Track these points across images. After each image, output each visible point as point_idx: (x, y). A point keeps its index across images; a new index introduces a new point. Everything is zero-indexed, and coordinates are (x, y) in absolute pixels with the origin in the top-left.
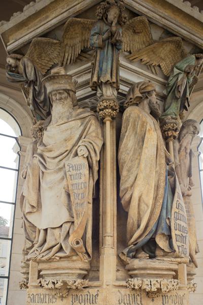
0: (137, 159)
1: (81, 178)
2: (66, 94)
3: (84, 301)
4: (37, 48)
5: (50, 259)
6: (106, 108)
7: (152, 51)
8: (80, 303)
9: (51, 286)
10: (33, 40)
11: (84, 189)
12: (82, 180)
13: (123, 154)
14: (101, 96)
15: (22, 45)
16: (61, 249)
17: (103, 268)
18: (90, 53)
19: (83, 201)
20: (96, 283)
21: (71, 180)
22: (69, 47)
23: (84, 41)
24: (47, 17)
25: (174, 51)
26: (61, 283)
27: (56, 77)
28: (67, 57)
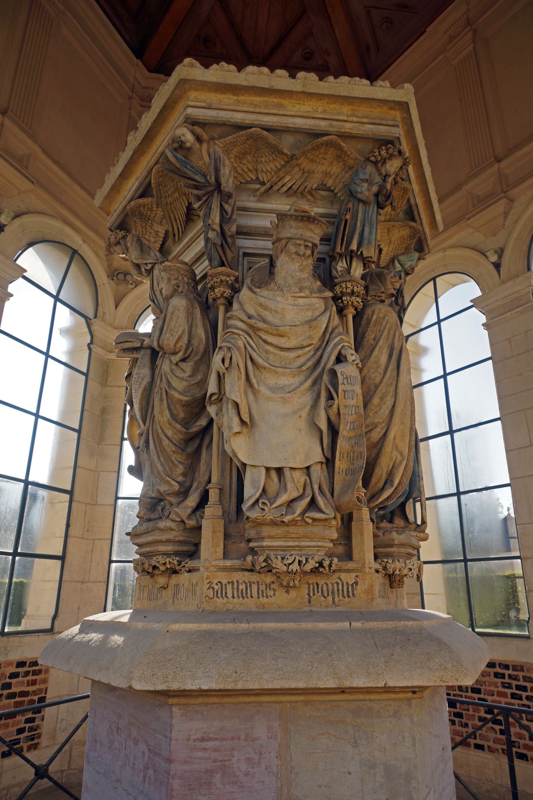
0: (392, 384)
1: (353, 399)
2: (309, 252)
4: (249, 142)
5: (292, 521)
6: (353, 293)
7: (388, 229)
8: (324, 597)
9: (295, 567)
11: (354, 416)
12: (353, 402)
13: (372, 371)
14: (341, 271)
16: (313, 504)
17: (363, 541)
20: (350, 565)
21: (345, 398)
22: (300, 169)
25: (404, 239)
26: (316, 562)
27: (316, 222)
28: (286, 180)
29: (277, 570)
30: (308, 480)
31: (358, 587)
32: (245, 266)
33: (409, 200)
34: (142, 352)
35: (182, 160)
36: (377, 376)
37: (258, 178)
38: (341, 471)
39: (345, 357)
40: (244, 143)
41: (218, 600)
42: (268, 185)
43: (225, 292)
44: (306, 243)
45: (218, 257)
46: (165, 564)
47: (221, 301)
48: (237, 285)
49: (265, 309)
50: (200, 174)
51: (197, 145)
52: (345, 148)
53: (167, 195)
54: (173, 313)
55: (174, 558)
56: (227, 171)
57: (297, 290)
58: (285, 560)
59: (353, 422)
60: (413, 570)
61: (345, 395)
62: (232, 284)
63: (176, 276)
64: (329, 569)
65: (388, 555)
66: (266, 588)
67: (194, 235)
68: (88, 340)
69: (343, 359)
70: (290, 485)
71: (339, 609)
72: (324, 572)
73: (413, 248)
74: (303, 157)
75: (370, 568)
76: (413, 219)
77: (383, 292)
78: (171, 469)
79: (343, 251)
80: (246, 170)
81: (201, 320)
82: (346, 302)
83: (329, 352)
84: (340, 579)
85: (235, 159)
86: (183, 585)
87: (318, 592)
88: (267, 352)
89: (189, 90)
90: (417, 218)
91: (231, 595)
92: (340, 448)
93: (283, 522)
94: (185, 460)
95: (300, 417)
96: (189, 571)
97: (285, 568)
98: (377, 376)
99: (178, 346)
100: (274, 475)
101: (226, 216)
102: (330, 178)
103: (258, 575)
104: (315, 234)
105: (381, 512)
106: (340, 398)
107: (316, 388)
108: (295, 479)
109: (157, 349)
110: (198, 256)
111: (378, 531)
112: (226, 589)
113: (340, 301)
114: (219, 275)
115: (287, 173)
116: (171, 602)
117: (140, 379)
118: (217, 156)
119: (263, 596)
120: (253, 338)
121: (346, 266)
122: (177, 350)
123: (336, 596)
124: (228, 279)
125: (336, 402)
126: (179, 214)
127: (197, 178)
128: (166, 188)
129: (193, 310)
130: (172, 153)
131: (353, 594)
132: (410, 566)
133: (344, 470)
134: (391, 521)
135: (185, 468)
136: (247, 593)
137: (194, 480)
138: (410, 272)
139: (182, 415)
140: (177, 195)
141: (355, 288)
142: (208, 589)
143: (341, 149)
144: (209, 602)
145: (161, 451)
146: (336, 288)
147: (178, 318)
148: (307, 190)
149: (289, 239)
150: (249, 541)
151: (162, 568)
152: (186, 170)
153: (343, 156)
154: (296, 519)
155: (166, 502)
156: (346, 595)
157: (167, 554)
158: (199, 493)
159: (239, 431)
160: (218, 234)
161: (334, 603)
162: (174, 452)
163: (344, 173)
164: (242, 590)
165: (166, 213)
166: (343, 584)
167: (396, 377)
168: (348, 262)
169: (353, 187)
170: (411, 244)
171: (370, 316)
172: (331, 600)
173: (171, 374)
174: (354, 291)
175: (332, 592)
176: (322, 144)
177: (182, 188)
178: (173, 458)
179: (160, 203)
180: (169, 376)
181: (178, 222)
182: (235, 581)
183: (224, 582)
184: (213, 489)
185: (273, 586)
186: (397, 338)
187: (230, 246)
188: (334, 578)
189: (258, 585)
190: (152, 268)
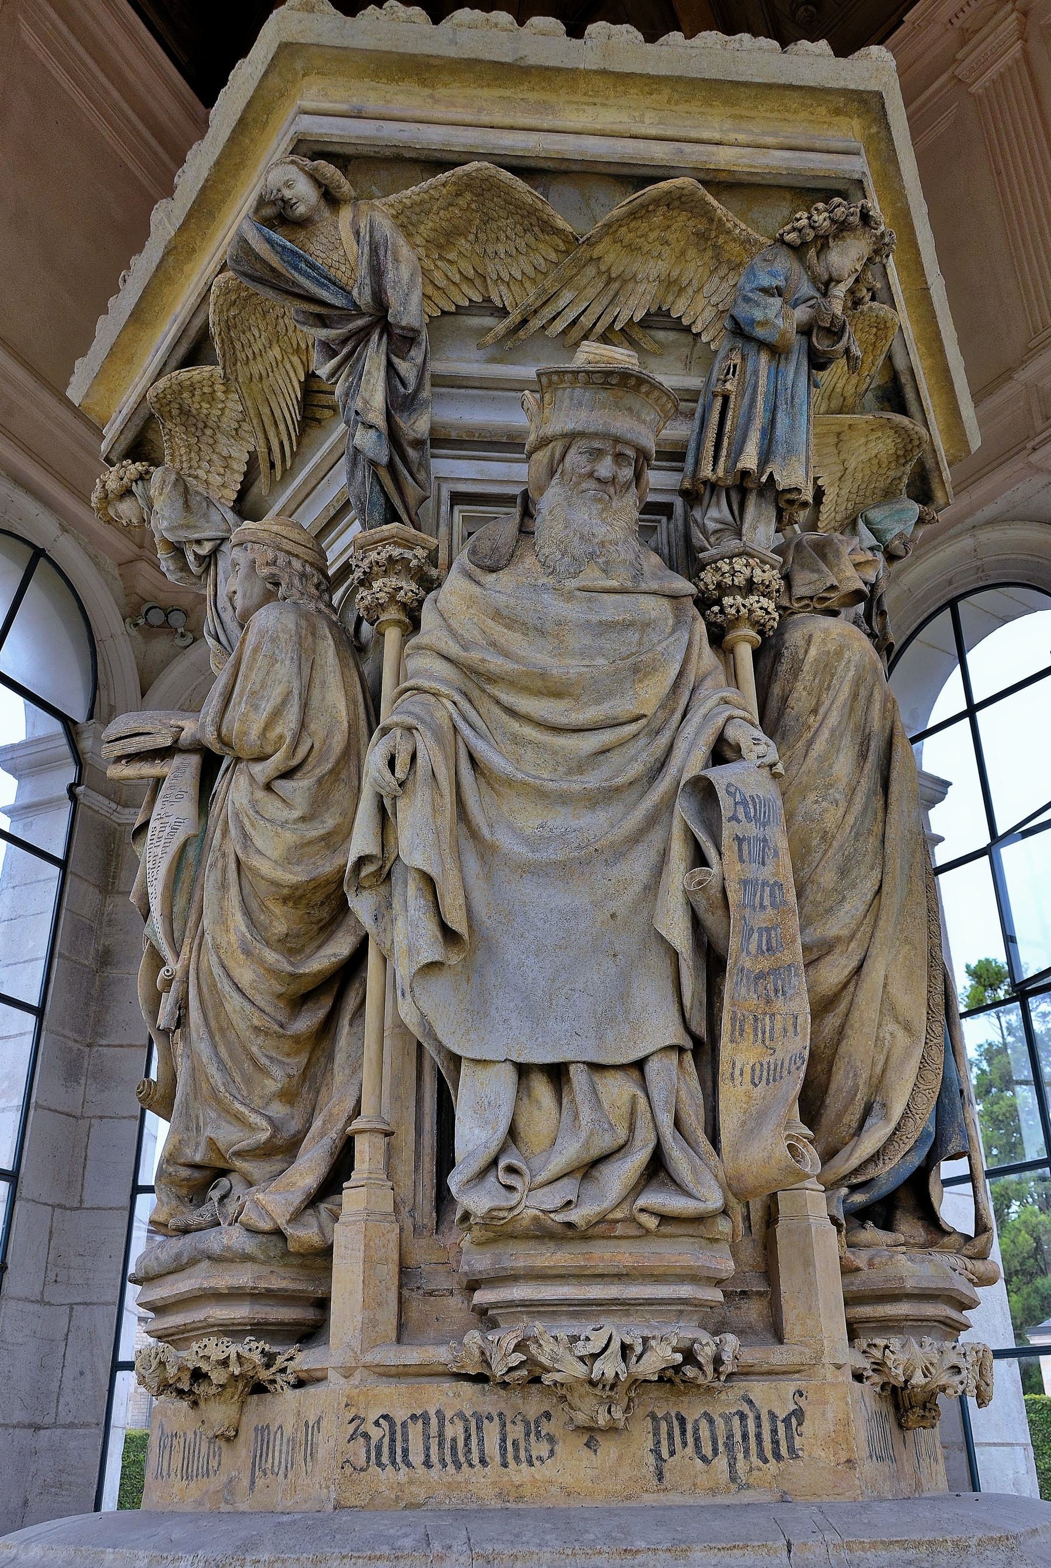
0: (870, 832)
1: (764, 864)
2: (628, 473)
3: (729, 1446)
4: (462, 202)
5: (598, 1223)
8: (704, 1459)
10: (475, 165)
11: (770, 911)
13: (812, 797)
14: (716, 532)
15: (388, 152)
16: (657, 1168)
17: (811, 1283)
18: (661, 335)
19: (765, 964)
20: (778, 1356)
22: (600, 273)
23: (672, 285)
24: (544, 107)
28: (562, 303)
29: (557, 1377)
30: (642, 1101)
31: (807, 1427)
32: (455, 529)
33: (890, 358)
34: (177, 760)
35: (284, 247)
36: (826, 810)
37: (487, 300)
38: (737, 1072)
39: (738, 749)
40: (452, 205)
41: (383, 1476)
42: (515, 317)
43: (401, 588)
44: (619, 448)
45: (382, 501)
46: (225, 1363)
47: (393, 613)
48: (434, 572)
49: (509, 627)
50: (334, 284)
51: (327, 213)
52: (719, 211)
53: (251, 357)
54: (256, 650)
55: (254, 1345)
56: (405, 273)
57: (597, 573)
58: (580, 1343)
59: (768, 930)
60: (964, 1372)
61: (740, 850)
62: (420, 568)
63: (270, 555)
64: (716, 1370)
65: (886, 1326)
66: (528, 1434)
67: (323, 459)
68: (70, 774)
69: (729, 754)
70: (586, 1114)
71: (748, 1496)
72: (701, 1380)
73: (904, 491)
74: (607, 239)
75: (839, 1367)
76: (902, 409)
77: (833, 588)
78: (248, 1081)
79: (720, 473)
80: (457, 278)
81: (338, 669)
82: (733, 611)
83: (691, 736)
84: (750, 1402)
85: (427, 249)
86: (281, 1427)
87: (685, 1444)
88: (516, 740)
89: (303, 76)
90: (913, 407)
91: (422, 1458)
92: (733, 1005)
93: (569, 1225)
94: (288, 1055)
95: (613, 916)
96: (300, 1384)
97: (580, 1370)
98: (826, 810)
99: (272, 735)
100: (542, 1089)
101: (402, 390)
102: (679, 295)
103: (502, 1392)
104: (644, 422)
105: (859, 1198)
106: (726, 858)
107: (656, 837)
108: (603, 1097)
109: (216, 748)
110: (332, 512)
111: (854, 1253)
112: (406, 1440)
113: (716, 609)
114: (384, 546)
115: (566, 283)
116: (246, 1482)
117: (168, 830)
118: (377, 236)
119: (517, 1458)
120: (476, 703)
121: (730, 518)
122: (269, 750)
123: (740, 1456)
124: (408, 554)
125: (715, 869)
126: (283, 405)
127: (324, 294)
128: (248, 334)
129: (314, 642)
130: (259, 230)
131: (791, 1449)
132: (953, 1359)
133: (748, 1069)
134: (887, 1226)
135: (289, 1076)
136: (469, 1451)
137: (317, 1112)
138: (901, 553)
139: (280, 928)
140: (276, 351)
141: (758, 571)
142: (352, 1438)
143: (708, 214)
144: (353, 1482)
145: (222, 1030)
146: (702, 575)
147: (273, 660)
148: (618, 327)
149: (571, 437)
150: (473, 1286)
151: (218, 1376)
152: (296, 275)
153: (713, 234)
154: (611, 1216)
155: (234, 1178)
156: (769, 1455)
157: (232, 1331)
158: (327, 1148)
159: (437, 958)
160: (379, 437)
161: (733, 1479)
162: (257, 1029)
163: (717, 280)
164: (454, 1440)
165: (249, 404)
166: (758, 1418)
167: (880, 815)
168: (735, 508)
169: (742, 311)
170: (900, 478)
171: (801, 652)
172: (726, 1467)
173: (251, 812)
174: (755, 580)
175: (726, 1445)
176: (656, 201)
177: (290, 333)
178: (254, 1049)
179: (232, 378)
180: (246, 820)
181: (282, 427)
182: (432, 1413)
183: (400, 1415)
184: (366, 1136)
185: (546, 1428)
186: (877, 706)
187: (415, 469)
188: (729, 1401)
189: (503, 1425)
190: (215, 553)
